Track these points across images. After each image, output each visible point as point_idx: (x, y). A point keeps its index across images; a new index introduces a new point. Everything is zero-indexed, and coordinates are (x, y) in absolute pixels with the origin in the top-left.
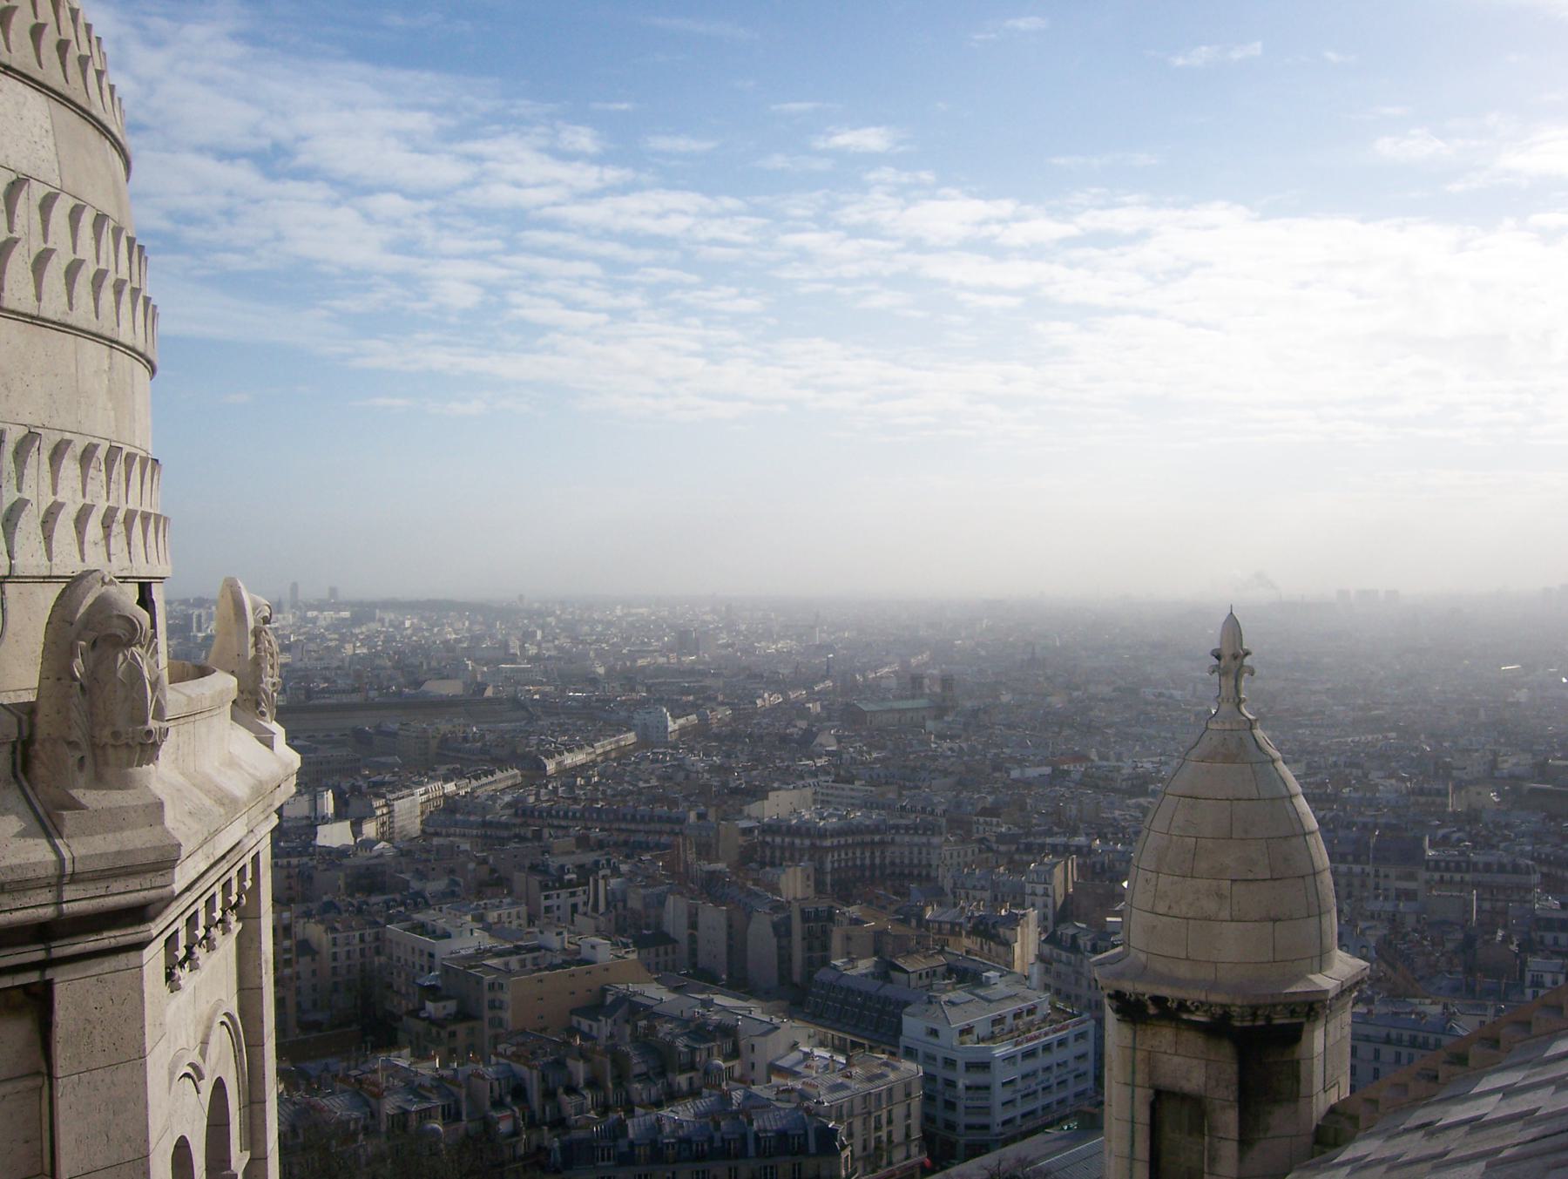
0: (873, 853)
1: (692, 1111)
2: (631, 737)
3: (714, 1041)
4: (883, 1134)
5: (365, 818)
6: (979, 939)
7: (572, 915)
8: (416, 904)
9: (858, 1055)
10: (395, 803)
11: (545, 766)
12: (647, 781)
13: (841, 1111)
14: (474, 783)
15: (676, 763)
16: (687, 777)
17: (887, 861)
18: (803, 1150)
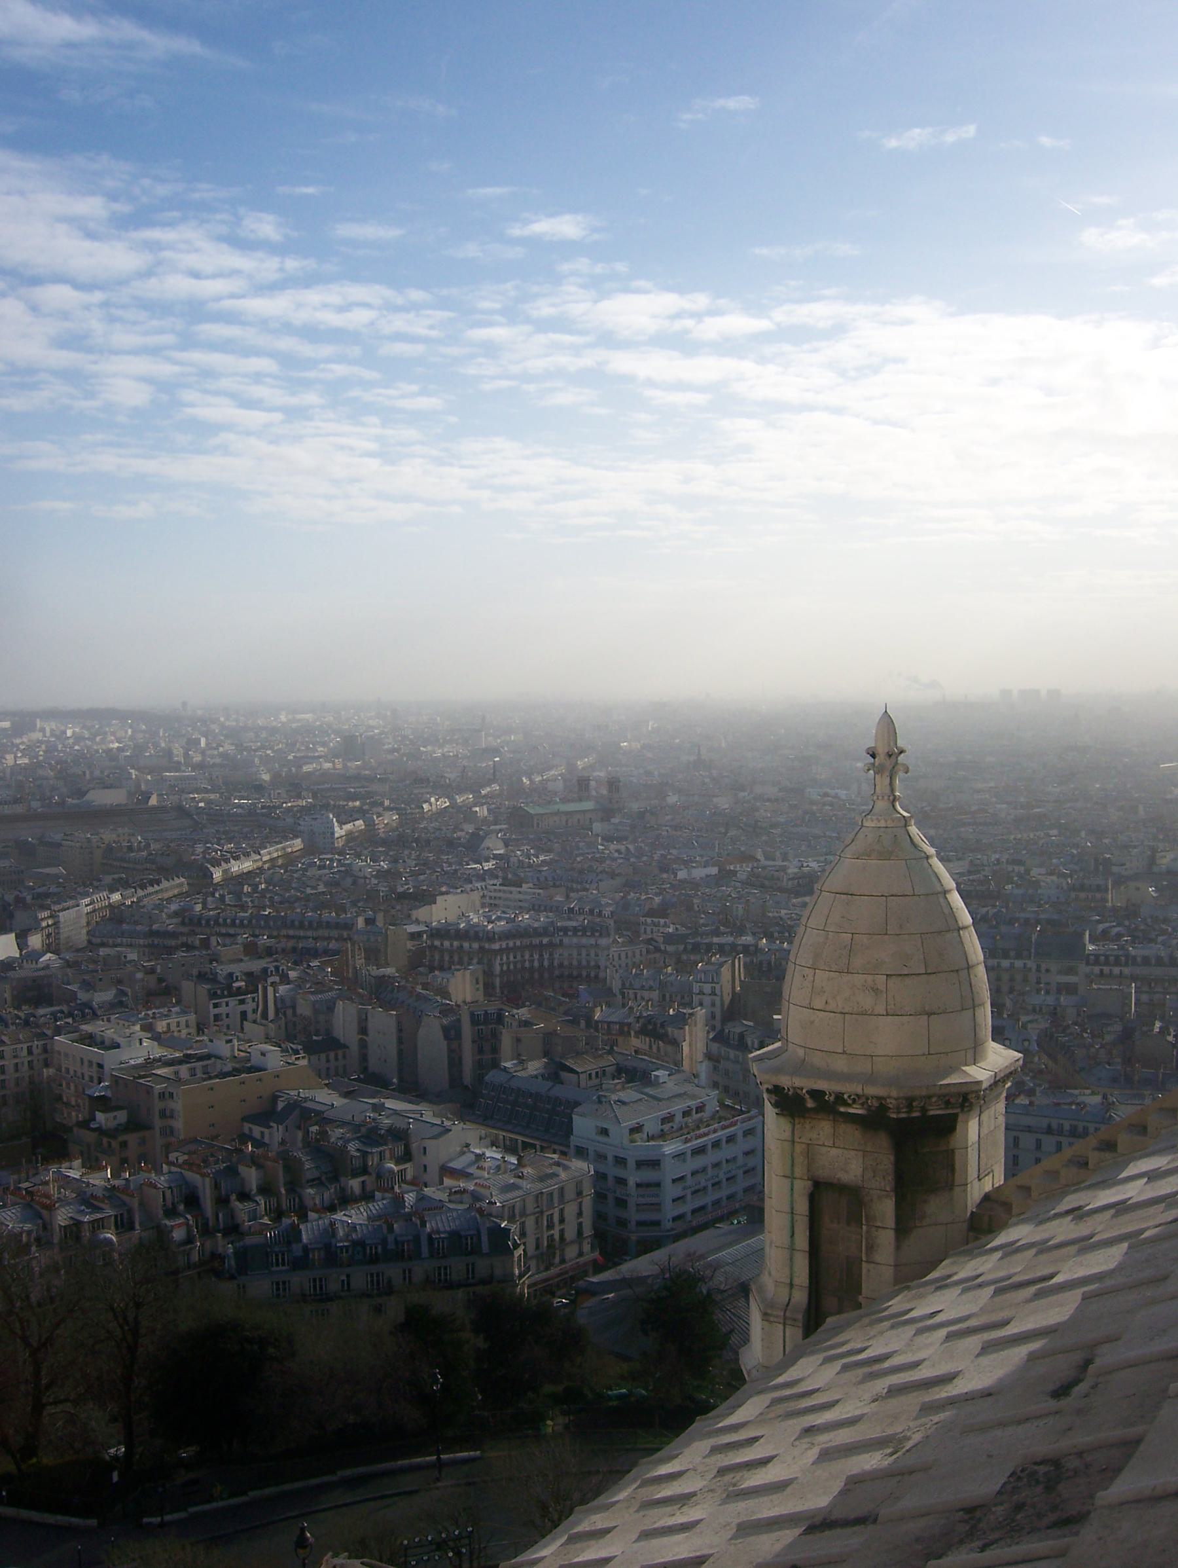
0: (541, 955)
1: (365, 1214)
2: (297, 844)
3: (386, 1144)
4: (556, 1233)
5: (30, 930)
6: (647, 1039)
7: (242, 1024)
8: (84, 1016)
9: (529, 1155)
10: (61, 914)
11: (212, 874)
12: (314, 888)
13: (513, 1211)
14: (140, 893)
15: (343, 869)
16: (354, 883)
17: (556, 963)
18: (475, 1251)
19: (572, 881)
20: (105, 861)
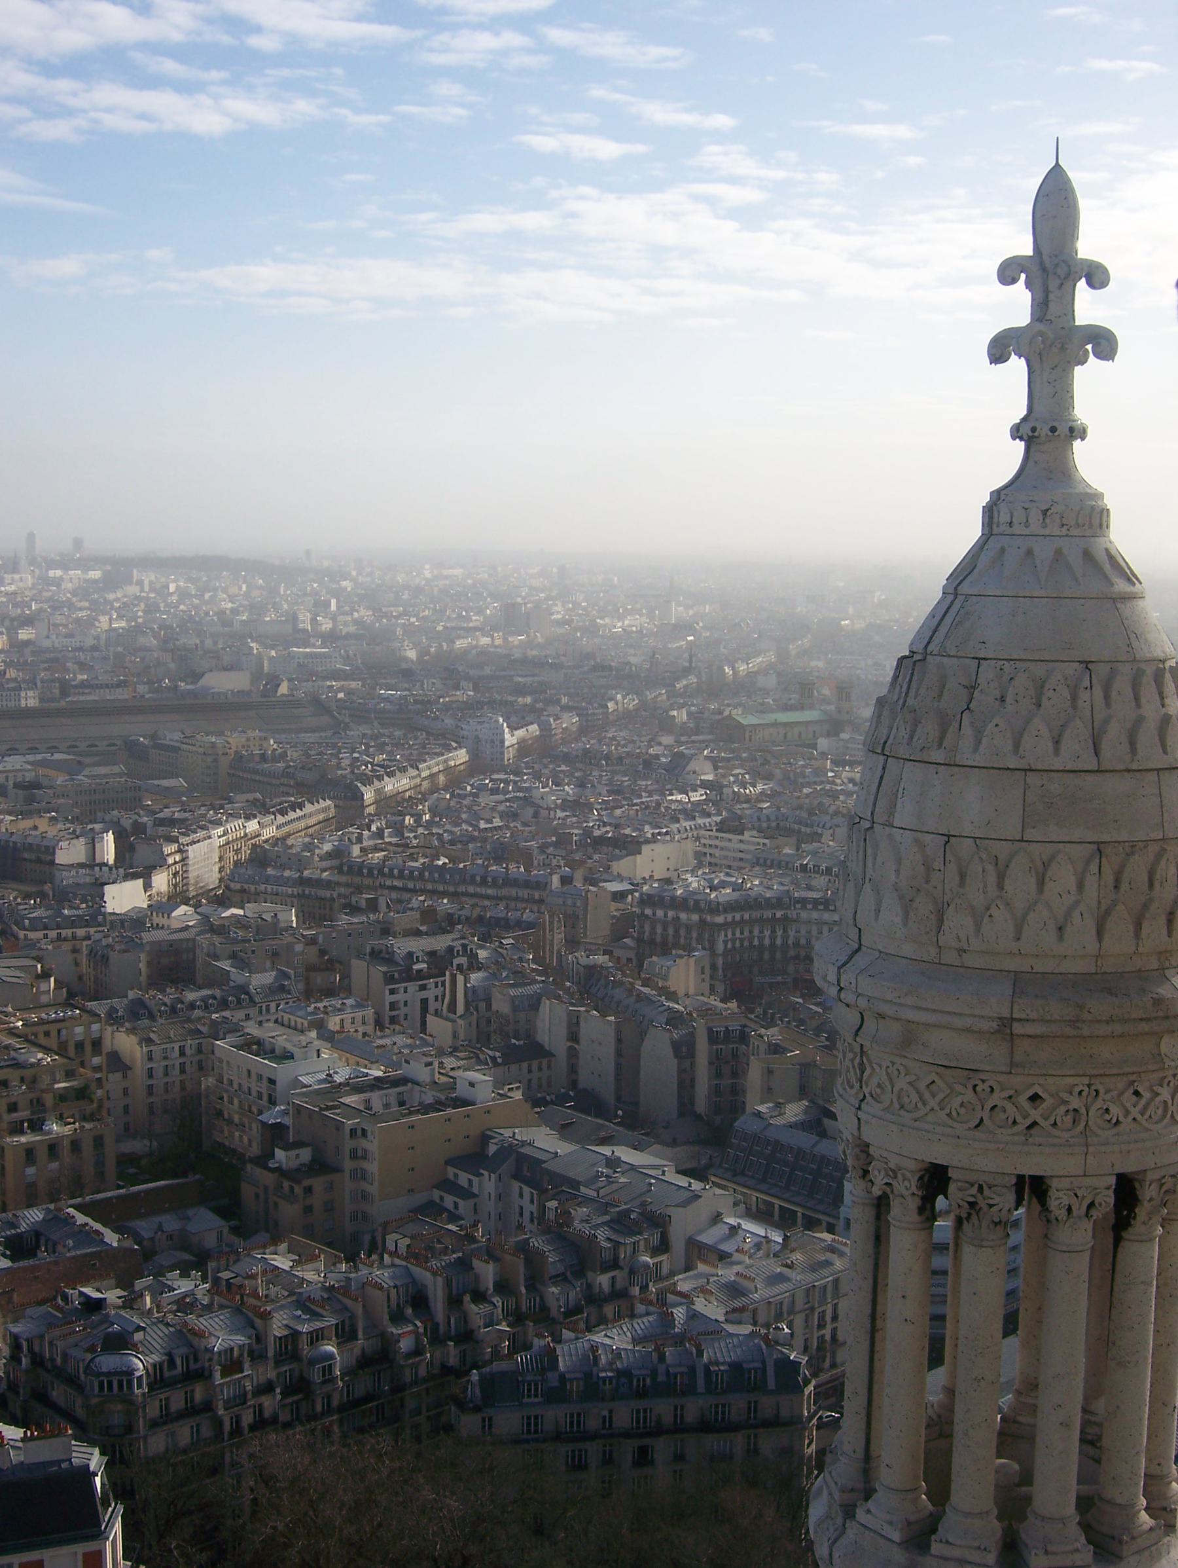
0: (773, 932)
1: (629, 1334)
2: (461, 756)
3: (640, 1233)
4: (827, 1332)
5: (155, 868)
8: (239, 1001)
9: (797, 1233)
10: (190, 848)
11: (363, 795)
12: (489, 821)
13: (781, 1308)
14: (281, 819)
15: (521, 795)
16: (536, 815)
17: (790, 942)
19: (800, 823)
20: (232, 772)
